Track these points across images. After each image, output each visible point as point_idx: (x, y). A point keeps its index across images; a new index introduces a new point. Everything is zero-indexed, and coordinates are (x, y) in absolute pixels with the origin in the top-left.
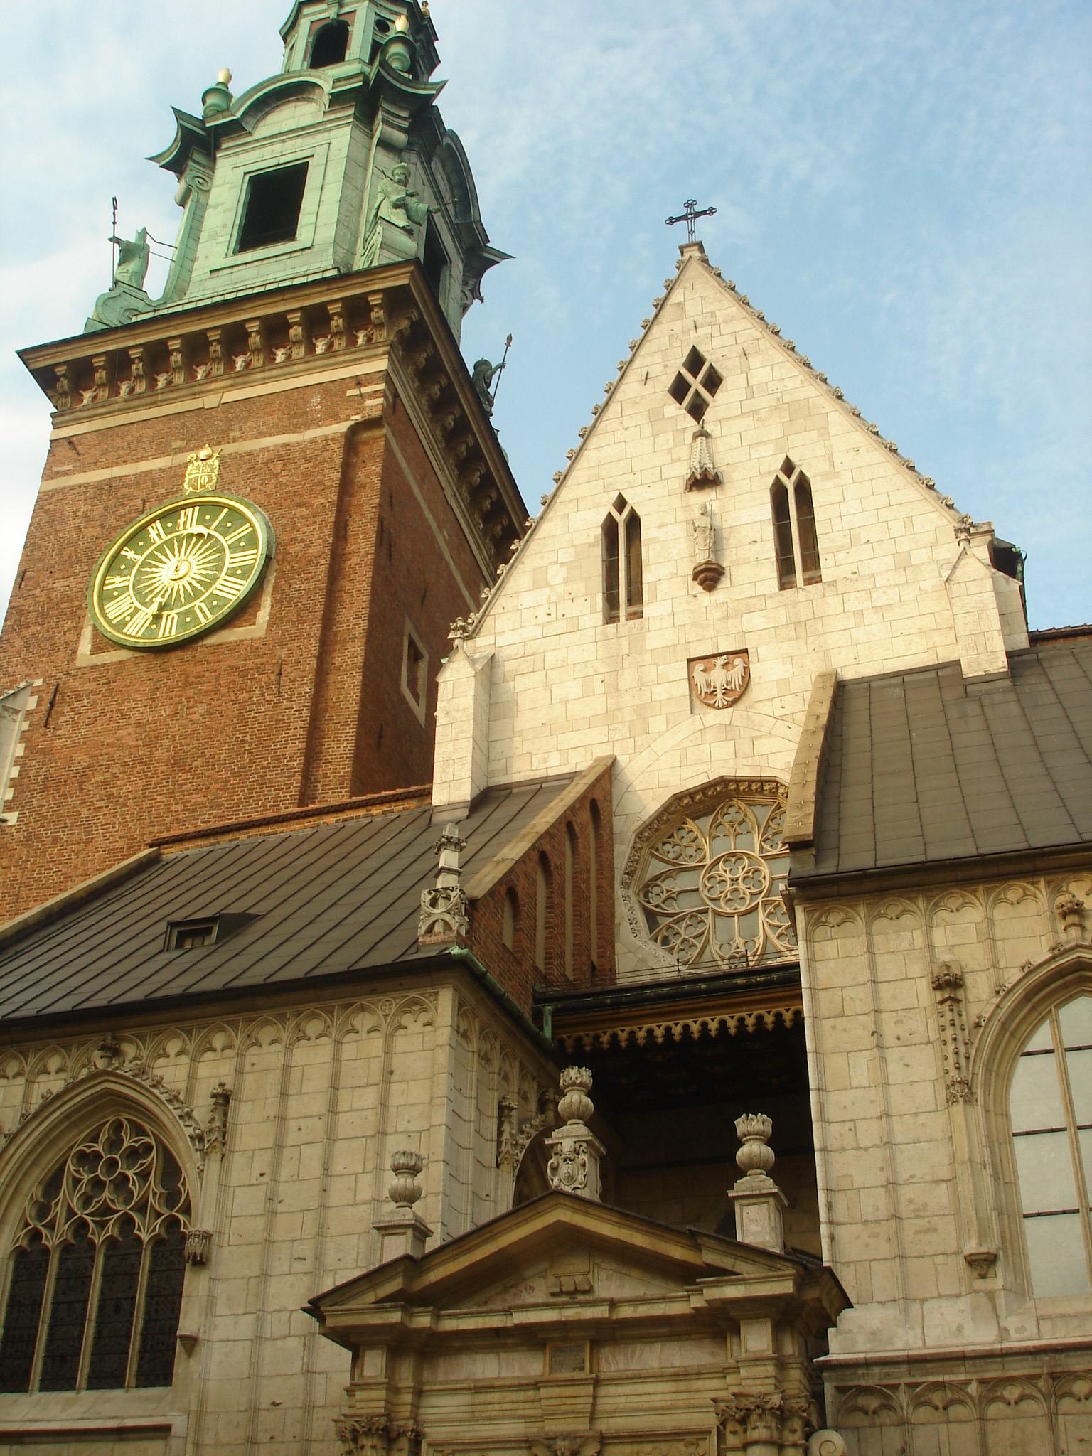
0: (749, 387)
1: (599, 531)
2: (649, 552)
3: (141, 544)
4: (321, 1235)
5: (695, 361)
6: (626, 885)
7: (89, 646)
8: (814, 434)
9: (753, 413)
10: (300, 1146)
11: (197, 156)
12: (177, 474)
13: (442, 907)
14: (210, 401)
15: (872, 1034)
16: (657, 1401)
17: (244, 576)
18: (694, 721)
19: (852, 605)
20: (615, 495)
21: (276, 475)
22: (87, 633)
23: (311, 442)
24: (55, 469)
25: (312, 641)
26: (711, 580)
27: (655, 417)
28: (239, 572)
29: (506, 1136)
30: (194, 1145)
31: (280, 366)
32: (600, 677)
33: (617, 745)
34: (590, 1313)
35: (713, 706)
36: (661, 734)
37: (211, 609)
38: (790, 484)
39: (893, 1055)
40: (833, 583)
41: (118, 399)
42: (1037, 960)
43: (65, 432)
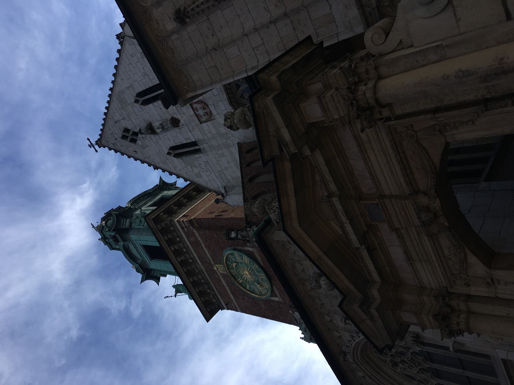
1: (179, 159)
3: (244, 285)
5: (124, 137)
7: (276, 298)
11: (153, 273)
12: (224, 276)
14: (203, 268)
17: (242, 256)
18: (217, 118)
22: (272, 298)
23: (202, 240)
24: (235, 308)
32: (217, 152)
33: (234, 143)
35: (211, 112)
41: (211, 292)
43: (225, 307)
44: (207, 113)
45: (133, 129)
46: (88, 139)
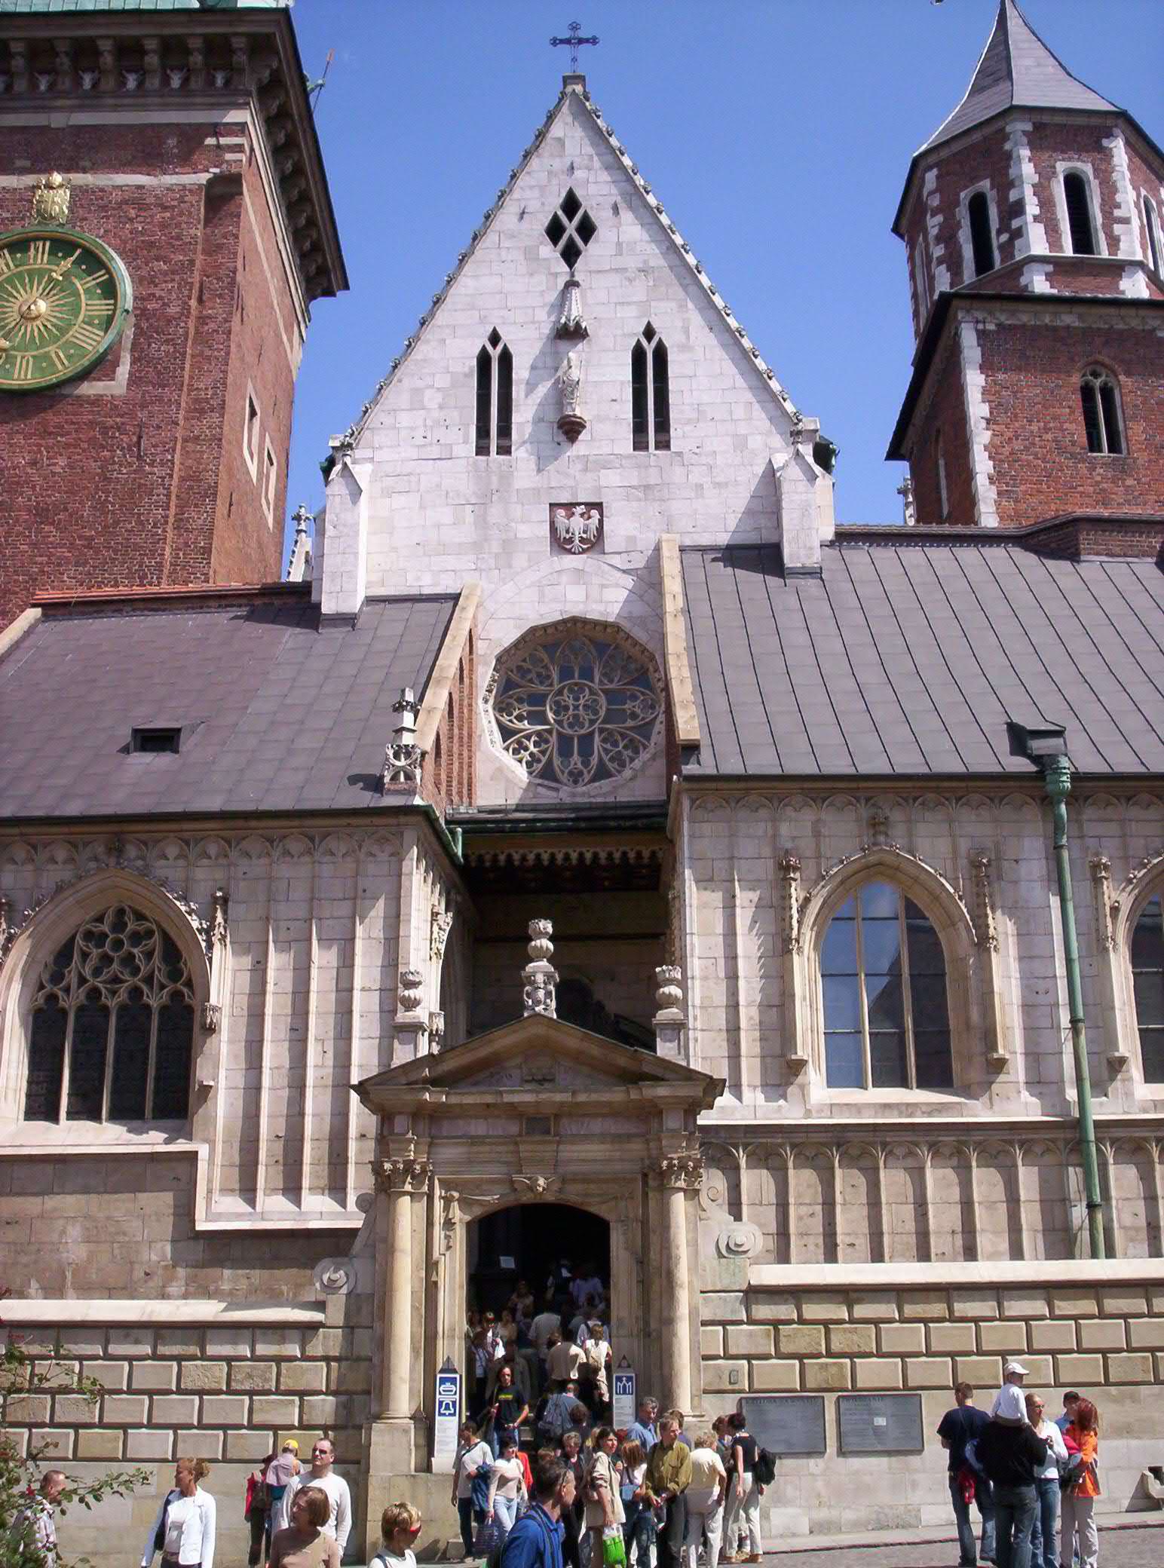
0: (619, 244)
1: (475, 362)
5: (571, 204)
6: (486, 701)
8: (673, 305)
10: (290, 942)
13: (402, 762)
16: (599, 1156)
19: (694, 478)
21: (131, 220)
23: (168, 189)
27: (531, 255)
28: (96, 322)
29: (435, 935)
31: (129, 95)
34: (558, 1097)
35: (570, 552)
36: (523, 570)
37: (69, 357)
38: (649, 349)
40: (680, 454)
44: (570, 541)
46: (594, 41)
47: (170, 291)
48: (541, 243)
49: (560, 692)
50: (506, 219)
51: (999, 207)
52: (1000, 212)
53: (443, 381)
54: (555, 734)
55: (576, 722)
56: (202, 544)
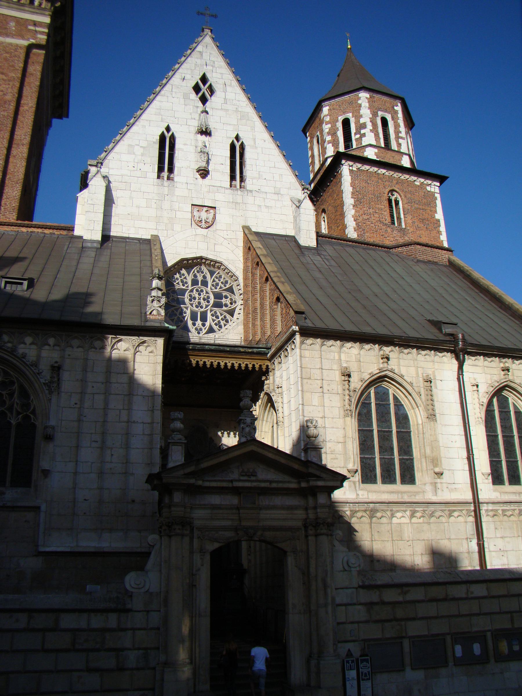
0: (225, 99)
2: (178, 154)
4: (104, 434)
5: (204, 79)
9: (226, 110)
10: (94, 394)
15: (321, 387)
20: (166, 125)
25: (5, 140)
26: (205, 174)
27: (186, 97)
30: (46, 387)
32: (155, 201)
35: (200, 226)
38: (238, 145)
39: (326, 396)
40: (251, 191)
42: (375, 373)
45: (211, 102)
47: (7, 89)
48: (191, 93)
49: (192, 291)
50: (176, 80)
51: (355, 124)
52: (356, 127)
53: (144, 144)
54: (189, 309)
55: (199, 305)
56: (14, 205)
